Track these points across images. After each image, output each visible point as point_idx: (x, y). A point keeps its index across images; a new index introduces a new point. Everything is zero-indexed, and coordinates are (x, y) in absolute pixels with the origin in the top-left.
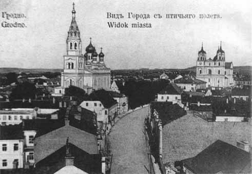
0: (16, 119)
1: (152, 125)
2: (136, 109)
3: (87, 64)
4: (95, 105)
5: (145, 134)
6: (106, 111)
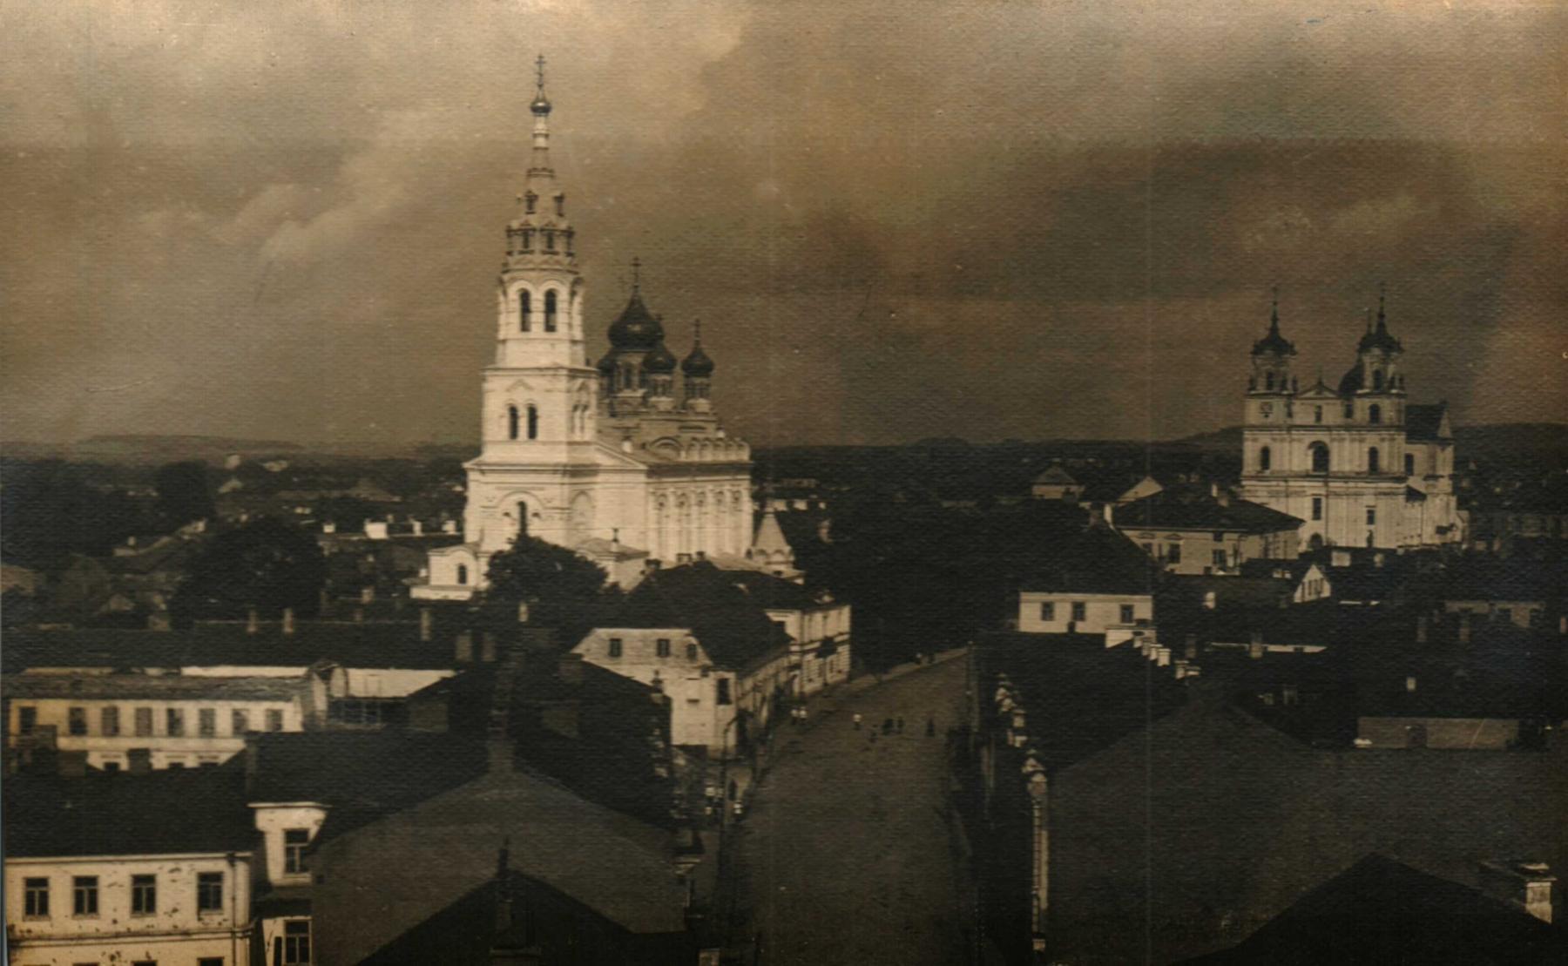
3: (613, 415)
4: (663, 648)
6: (722, 685)
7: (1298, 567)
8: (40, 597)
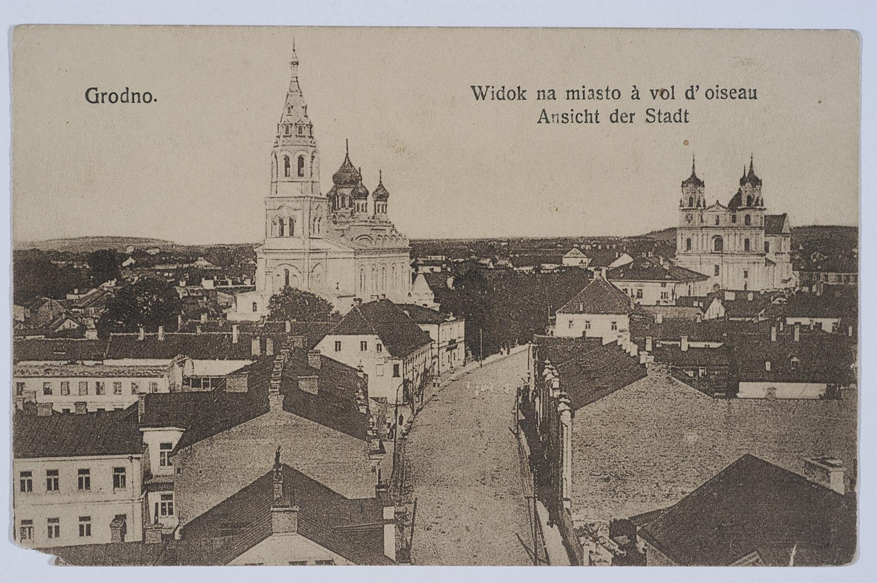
0: (117, 390)
1: (538, 407)
2: (489, 359)
3: (335, 223)
4: (364, 346)
5: (517, 435)
6: (396, 367)
7: (706, 302)
8: (27, 321)
